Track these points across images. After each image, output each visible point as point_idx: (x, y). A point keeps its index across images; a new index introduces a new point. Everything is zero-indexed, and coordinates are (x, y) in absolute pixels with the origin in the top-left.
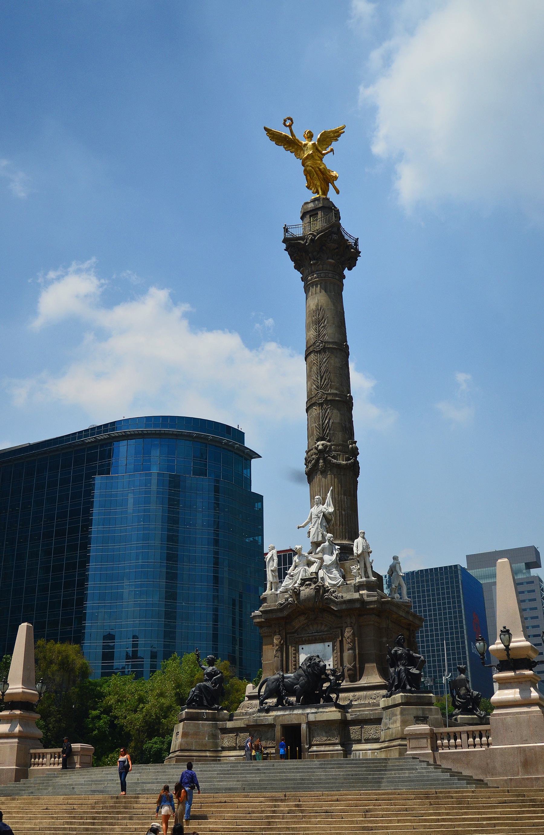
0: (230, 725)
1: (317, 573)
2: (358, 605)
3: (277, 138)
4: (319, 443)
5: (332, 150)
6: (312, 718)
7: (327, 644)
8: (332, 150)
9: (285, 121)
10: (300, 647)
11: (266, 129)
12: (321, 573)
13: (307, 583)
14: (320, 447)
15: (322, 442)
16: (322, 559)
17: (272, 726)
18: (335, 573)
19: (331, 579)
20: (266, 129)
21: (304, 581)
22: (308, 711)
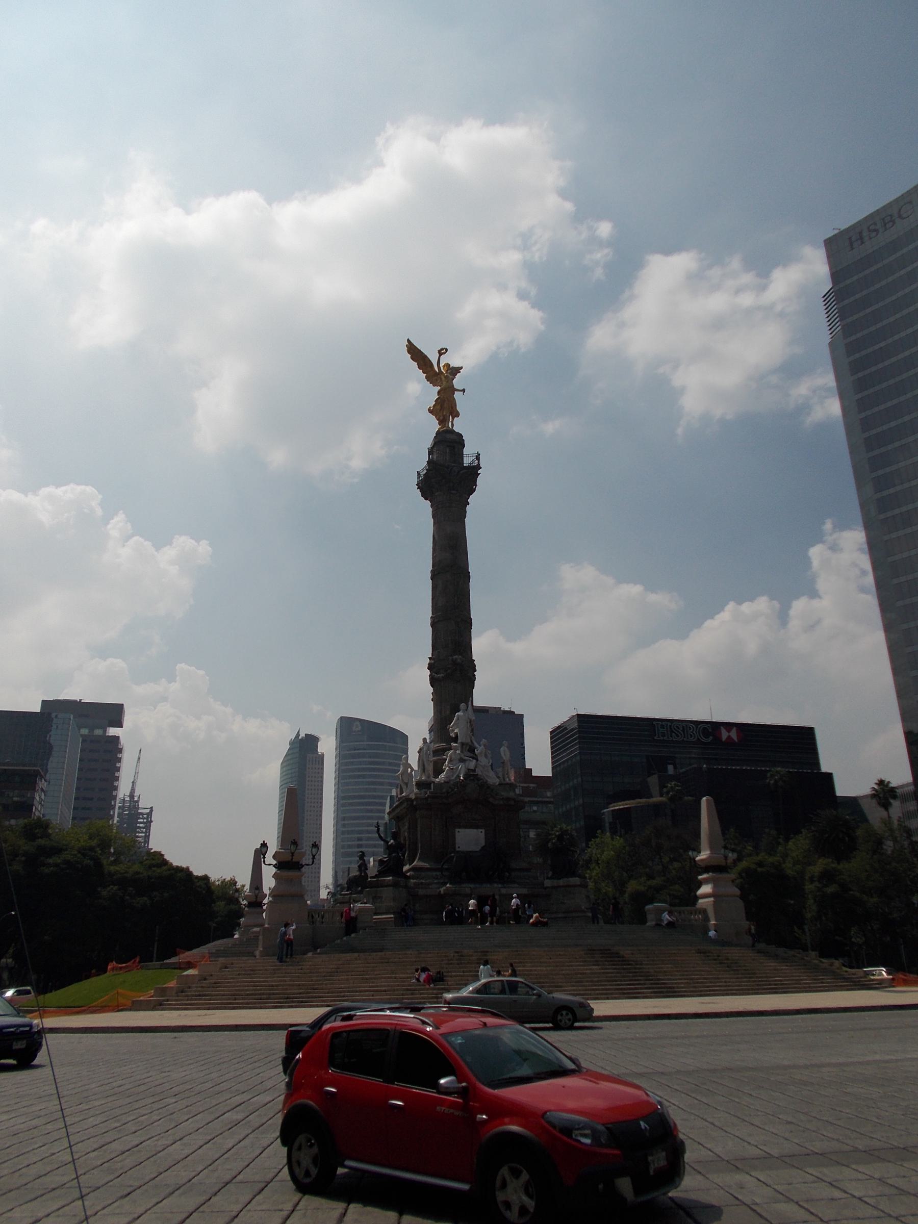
0: (421, 892)
2: (512, 803)
3: (415, 353)
5: (464, 391)
6: (504, 891)
8: (464, 391)
9: (442, 349)
10: (457, 830)
12: (479, 772)
14: (459, 661)
22: (496, 885)
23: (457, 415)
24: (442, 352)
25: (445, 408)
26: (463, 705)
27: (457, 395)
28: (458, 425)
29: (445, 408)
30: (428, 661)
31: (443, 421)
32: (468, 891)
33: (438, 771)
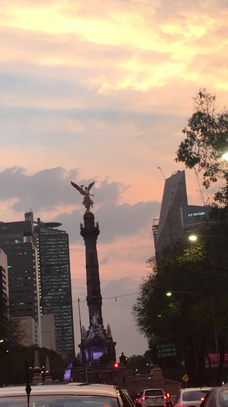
0: (80, 373)
1: (98, 335)
4: (93, 297)
5: (93, 195)
6: (103, 372)
7: (100, 353)
8: (93, 195)
11: (71, 182)
13: (96, 338)
14: (94, 298)
15: (95, 296)
16: (98, 331)
17: (93, 374)
18: (103, 335)
19: (102, 336)
20: (71, 182)
21: (95, 337)
23: (93, 204)
24: (82, 186)
25: (88, 203)
26: (95, 314)
27: (91, 198)
28: (93, 210)
29: (88, 203)
30: (86, 297)
31: (88, 207)
32: (93, 372)
33: (88, 336)
